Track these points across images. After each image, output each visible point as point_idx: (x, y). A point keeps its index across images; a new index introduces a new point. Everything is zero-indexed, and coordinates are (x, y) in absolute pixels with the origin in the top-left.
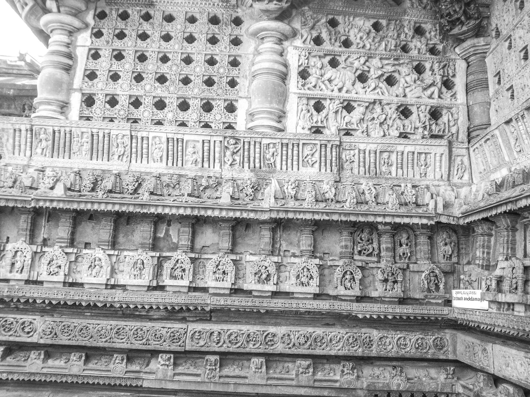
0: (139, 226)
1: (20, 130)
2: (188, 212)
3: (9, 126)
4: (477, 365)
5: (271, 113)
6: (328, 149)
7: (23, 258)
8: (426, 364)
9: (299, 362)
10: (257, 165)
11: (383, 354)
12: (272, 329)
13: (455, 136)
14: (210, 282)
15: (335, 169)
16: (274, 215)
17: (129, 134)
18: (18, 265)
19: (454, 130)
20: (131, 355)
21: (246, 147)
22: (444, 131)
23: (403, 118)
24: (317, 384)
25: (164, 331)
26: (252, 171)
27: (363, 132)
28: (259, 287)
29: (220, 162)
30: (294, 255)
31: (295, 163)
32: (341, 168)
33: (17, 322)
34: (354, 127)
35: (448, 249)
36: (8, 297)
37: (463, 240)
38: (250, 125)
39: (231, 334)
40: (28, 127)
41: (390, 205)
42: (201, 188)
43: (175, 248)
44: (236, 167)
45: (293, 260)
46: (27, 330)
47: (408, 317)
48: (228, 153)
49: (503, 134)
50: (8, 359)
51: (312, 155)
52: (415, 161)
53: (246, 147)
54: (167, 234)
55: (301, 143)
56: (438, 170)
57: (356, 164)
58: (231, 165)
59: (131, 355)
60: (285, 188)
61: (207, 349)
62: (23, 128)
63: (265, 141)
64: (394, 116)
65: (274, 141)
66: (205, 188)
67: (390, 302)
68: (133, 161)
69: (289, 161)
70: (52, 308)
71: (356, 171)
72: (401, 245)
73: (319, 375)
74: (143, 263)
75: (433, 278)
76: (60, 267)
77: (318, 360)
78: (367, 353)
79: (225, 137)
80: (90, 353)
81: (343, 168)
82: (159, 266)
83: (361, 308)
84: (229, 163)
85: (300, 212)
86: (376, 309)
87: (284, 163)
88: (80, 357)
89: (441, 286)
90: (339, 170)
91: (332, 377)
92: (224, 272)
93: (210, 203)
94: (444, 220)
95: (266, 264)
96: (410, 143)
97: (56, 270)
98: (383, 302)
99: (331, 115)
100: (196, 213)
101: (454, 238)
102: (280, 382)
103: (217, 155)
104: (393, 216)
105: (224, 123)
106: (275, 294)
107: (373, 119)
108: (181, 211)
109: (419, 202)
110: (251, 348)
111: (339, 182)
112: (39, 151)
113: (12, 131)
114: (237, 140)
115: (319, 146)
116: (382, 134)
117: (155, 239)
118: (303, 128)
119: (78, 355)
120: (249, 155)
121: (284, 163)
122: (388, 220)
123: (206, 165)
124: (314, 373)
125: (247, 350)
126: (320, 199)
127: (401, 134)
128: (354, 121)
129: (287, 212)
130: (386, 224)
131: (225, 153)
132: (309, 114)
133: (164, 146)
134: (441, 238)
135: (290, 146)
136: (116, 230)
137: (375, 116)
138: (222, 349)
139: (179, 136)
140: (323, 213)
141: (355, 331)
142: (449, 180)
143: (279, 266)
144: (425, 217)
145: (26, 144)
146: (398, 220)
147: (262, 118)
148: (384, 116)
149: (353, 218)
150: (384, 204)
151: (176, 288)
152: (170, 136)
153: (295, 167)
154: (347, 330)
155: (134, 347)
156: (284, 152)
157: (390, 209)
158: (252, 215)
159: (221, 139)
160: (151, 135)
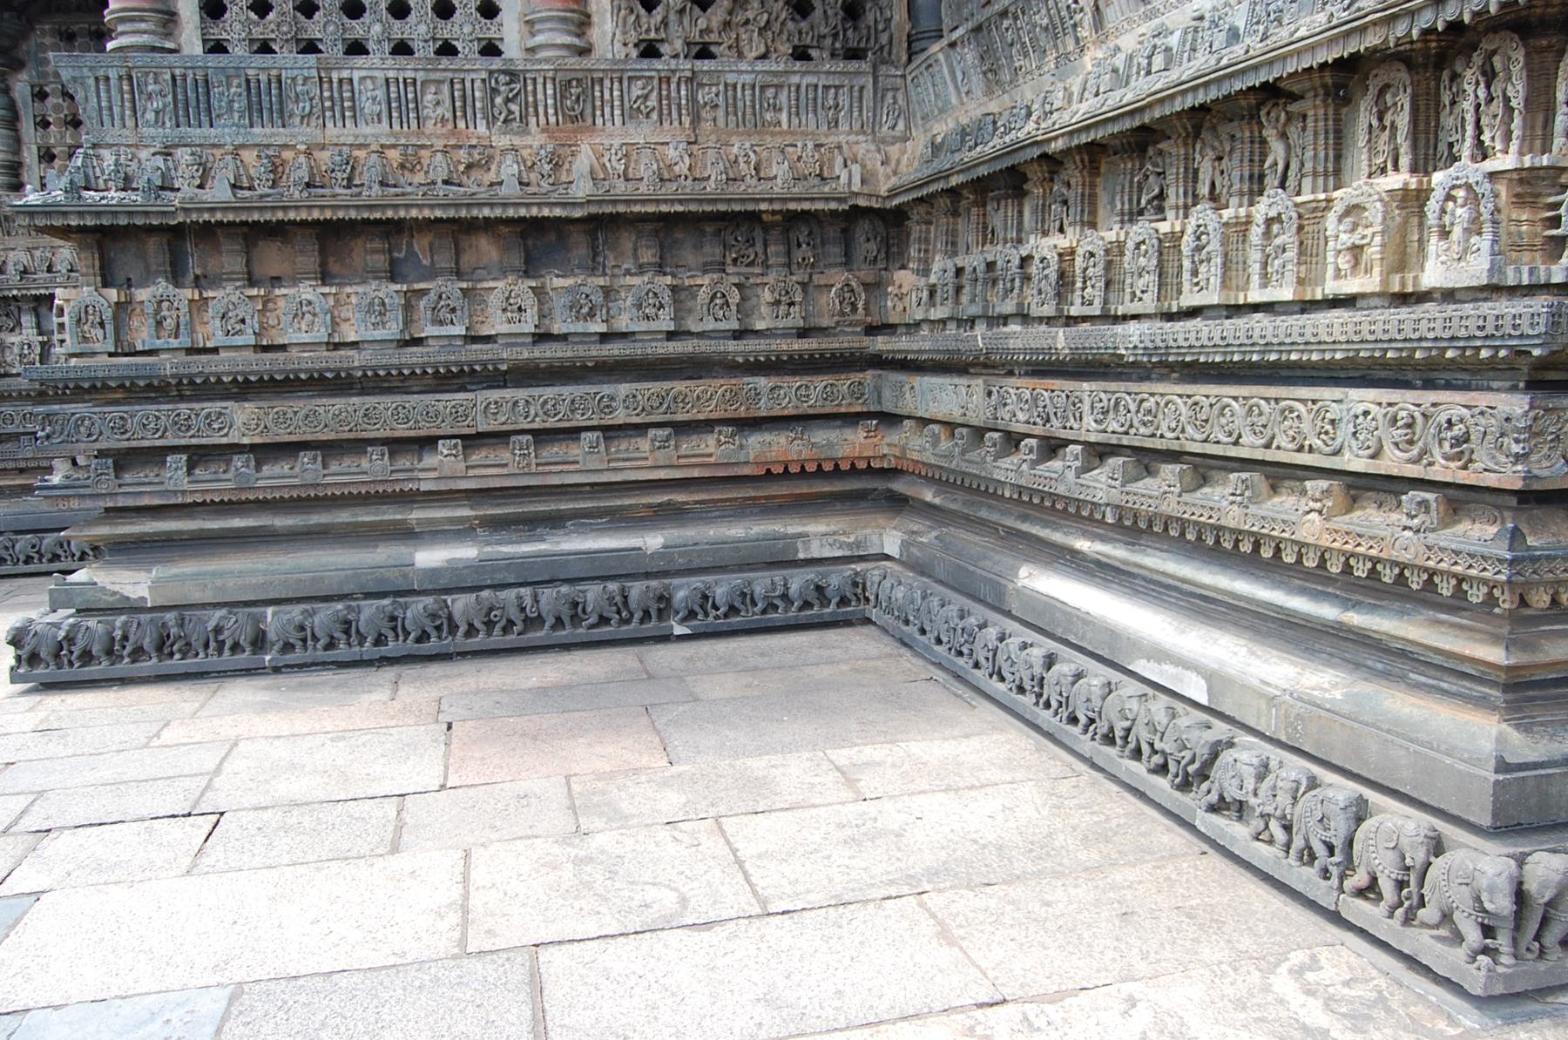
0: (360, 242)
1: (107, 79)
2: (451, 213)
3: (86, 71)
4: (904, 412)
5: (564, 20)
6: (673, 86)
7: (174, 313)
8: (839, 423)
9: (652, 432)
10: (552, 120)
11: (776, 412)
12: (606, 389)
13: (886, 49)
14: (496, 324)
15: (686, 121)
16: (594, 209)
17: (314, 73)
18: (169, 323)
19: (884, 39)
20: (396, 445)
21: (530, 88)
22: (868, 40)
23: (798, 17)
24: (682, 461)
25: (441, 406)
26: (543, 131)
27: (730, 47)
28: (579, 327)
29: (486, 117)
30: (628, 273)
31: (617, 112)
32: (696, 120)
33: (197, 415)
34: (714, 37)
35: (872, 246)
36: (172, 376)
37: (893, 232)
38: (531, 43)
39: (545, 402)
40: (123, 72)
41: (779, 181)
42: (462, 168)
43: (432, 274)
44: (515, 125)
45: (629, 280)
46: (216, 426)
47: (811, 356)
48: (499, 100)
49: (947, 57)
50: (197, 471)
51: (646, 97)
52: (820, 101)
53: (530, 88)
54: (411, 253)
55: (625, 76)
56: (856, 114)
57: (721, 113)
58: (505, 121)
59: (396, 445)
60: (606, 159)
61: (511, 428)
62: (113, 74)
63: (559, 76)
64: (784, 15)
65: (580, 75)
66: (469, 167)
67: (784, 336)
68: (330, 124)
69: (607, 110)
70: (244, 389)
71: (721, 122)
72: (799, 245)
73: (684, 448)
74: (383, 304)
75: (847, 295)
76: (243, 321)
77: (684, 428)
78: (753, 414)
79: (491, 73)
80: (330, 449)
81: (699, 117)
82: (408, 308)
83: (741, 348)
84: (502, 118)
85: (636, 202)
86: (763, 347)
87: (598, 113)
88: (315, 458)
89: (860, 305)
90: (692, 122)
91: (703, 449)
92: (520, 309)
93: (483, 195)
94: (862, 202)
95: (587, 290)
96: (811, 68)
97: (238, 327)
98: (775, 336)
99: (673, 17)
100: (463, 213)
101: (881, 229)
102: (627, 464)
103: (478, 105)
104: (785, 200)
105: (479, 40)
106: (604, 337)
107: (747, 22)
108: (439, 213)
109: (826, 174)
110: (579, 420)
111: (695, 143)
112: (150, 116)
113: (91, 81)
114: (513, 75)
115: (656, 82)
116: (762, 49)
117: (393, 262)
118: (625, 44)
119: (310, 454)
120: (535, 101)
121: (598, 113)
122: (777, 206)
123: (461, 124)
124: (677, 447)
125: (573, 424)
126: (666, 176)
127: (795, 48)
128: (715, 25)
129: (614, 202)
130: (774, 212)
131: (492, 100)
132: (633, 18)
133: (380, 94)
134: (862, 228)
135: (607, 83)
136: (323, 252)
137: (750, 15)
138: (535, 426)
139: (409, 74)
140: (672, 201)
141: (734, 381)
142: (873, 131)
143: (607, 292)
144: (834, 199)
145: (122, 106)
146: (792, 206)
147: (551, 30)
148: (765, 16)
149: (722, 207)
150: (770, 179)
151: (442, 337)
152: (391, 74)
153: (618, 120)
154: (722, 381)
155: (397, 434)
156: (597, 94)
157: (778, 188)
158: (558, 212)
159: (484, 75)
160: (356, 75)
